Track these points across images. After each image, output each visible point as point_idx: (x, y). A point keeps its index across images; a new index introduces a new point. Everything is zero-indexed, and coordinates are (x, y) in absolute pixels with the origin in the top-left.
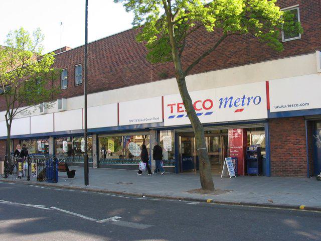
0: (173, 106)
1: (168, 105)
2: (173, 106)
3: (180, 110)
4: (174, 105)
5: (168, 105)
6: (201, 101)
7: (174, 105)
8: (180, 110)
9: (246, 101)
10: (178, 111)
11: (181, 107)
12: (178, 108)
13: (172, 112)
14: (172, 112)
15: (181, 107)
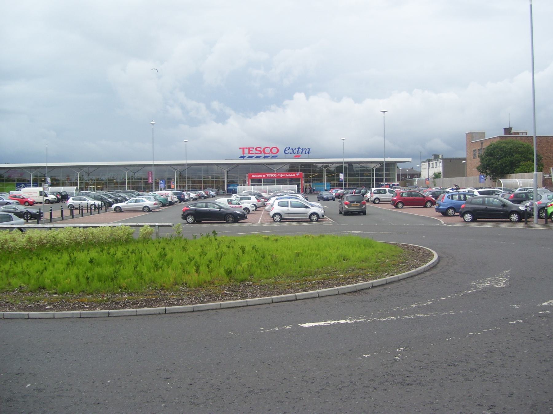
0: (245, 149)
1: (240, 148)
2: (245, 149)
3: (251, 152)
4: (247, 148)
5: (240, 148)
6: (269, 148)
7: (247, 148)
8: (251, 152)
9: (300, 151)
10: (249, 153)
11: (252, 151)
12: (249, 151)
13: (244, 153)
14: (244, 153)
15: (252, 151)
